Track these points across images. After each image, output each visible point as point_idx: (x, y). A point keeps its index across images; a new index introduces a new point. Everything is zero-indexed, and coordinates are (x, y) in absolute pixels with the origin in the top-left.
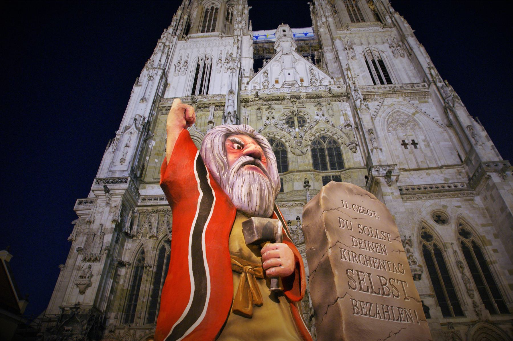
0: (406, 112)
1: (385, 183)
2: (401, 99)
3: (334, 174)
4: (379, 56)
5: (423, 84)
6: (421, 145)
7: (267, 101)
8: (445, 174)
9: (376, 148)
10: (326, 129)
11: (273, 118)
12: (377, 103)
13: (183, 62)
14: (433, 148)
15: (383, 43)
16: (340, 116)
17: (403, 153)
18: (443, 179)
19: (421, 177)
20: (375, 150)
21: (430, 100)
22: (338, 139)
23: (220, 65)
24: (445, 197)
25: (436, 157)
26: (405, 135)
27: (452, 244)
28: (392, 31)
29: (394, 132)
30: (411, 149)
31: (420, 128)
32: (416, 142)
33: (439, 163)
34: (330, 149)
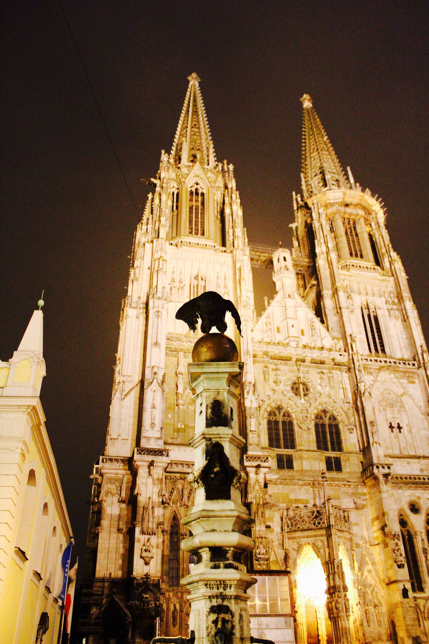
1: (383, 481)
2: (392, 376)
3: (335, 455)
4: (374, 310)
6: (405, 430)
7: (274, 359)
8: (421, 464)
9: (376, 443)
13: (177, 280)
14: (414, 436)
15: (381, 296)
16: (340, 388)
17: (390, 437)
18: (419, 469)
19: (403, 465)
20: (375, 444)
21: (417, 381)
22: (338, 415)
24: (420, 489)
25: (416, 445)
26: (393, 417)
27: (421, 532)
28: (389, 281)
29: (383, 412)
30: (397, 434)
32: (401, 426)
33: (417, 451)
34: (330, 425)
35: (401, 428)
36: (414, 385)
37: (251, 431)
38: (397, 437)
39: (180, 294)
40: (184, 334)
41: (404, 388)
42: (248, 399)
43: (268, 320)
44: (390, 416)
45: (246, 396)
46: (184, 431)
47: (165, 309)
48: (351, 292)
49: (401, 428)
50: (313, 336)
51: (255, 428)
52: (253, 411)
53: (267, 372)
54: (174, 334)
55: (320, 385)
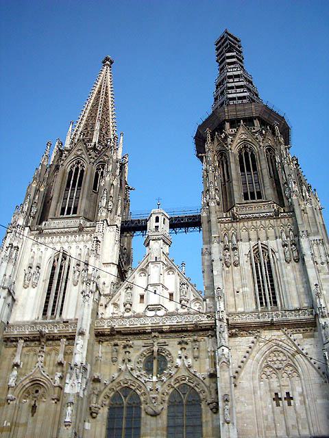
10: (187, 378)
11: (129, 361)
12: (252, 338)
13: (34, 265)
17: (273, 412)
23: (77, 273)
26: (280, 386)
31: (299, 376)
32: (291, 396)
35: (292, 398)
36: (313, 339)
37: (65, 422)
38: (283, 412)
42: (69, 385)
43: (129, 291)
44: (275, 385)
46: (10, 429)
48: (237, 241)
49: (292, 398)
51: (71, 418)
52: (71, 399)
55: (180, 358)
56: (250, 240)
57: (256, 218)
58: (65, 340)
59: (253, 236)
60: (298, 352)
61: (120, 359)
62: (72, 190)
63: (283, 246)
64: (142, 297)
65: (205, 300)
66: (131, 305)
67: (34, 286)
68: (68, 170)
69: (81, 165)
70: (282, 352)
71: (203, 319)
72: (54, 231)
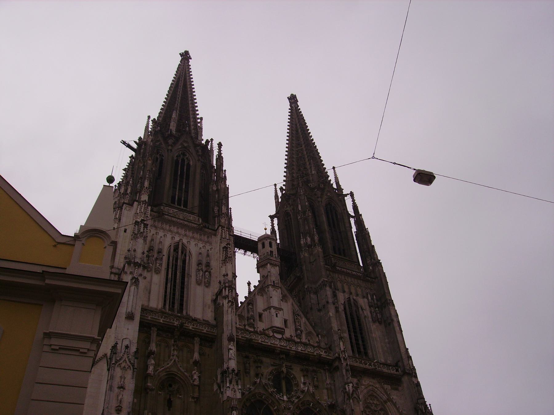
0: (379, 397)
5: (397, 368)
10: (312, 404)
11: (262, 375)
12: (355, 380)
13: (156, 249)
15: (364, 297)
39: (158, 265)
40: (158, 309)
41: (388, 395)
42: (231, 389)
43: (250, 306)
45: (228, 385)
47: (143, 276)
50: (296, 330)
52: (234, 403)
53: (248, 362)
54: (148, 306)
55: (304, 384)
56: (344, 292)
57: (348, 274)
58: (199, 339)
59: (346, 289)
60: (390, 400)
61: (252, 373)
62: (181, 182)
63: (370, 307)
64: (260, 315)
65: (318, 336)
66: (254, 321)
67: (158, 272)
68: (175, 158)
69: (187, 158)
70: (376, 397)
71: (321, 353)
72: (174, 219)
